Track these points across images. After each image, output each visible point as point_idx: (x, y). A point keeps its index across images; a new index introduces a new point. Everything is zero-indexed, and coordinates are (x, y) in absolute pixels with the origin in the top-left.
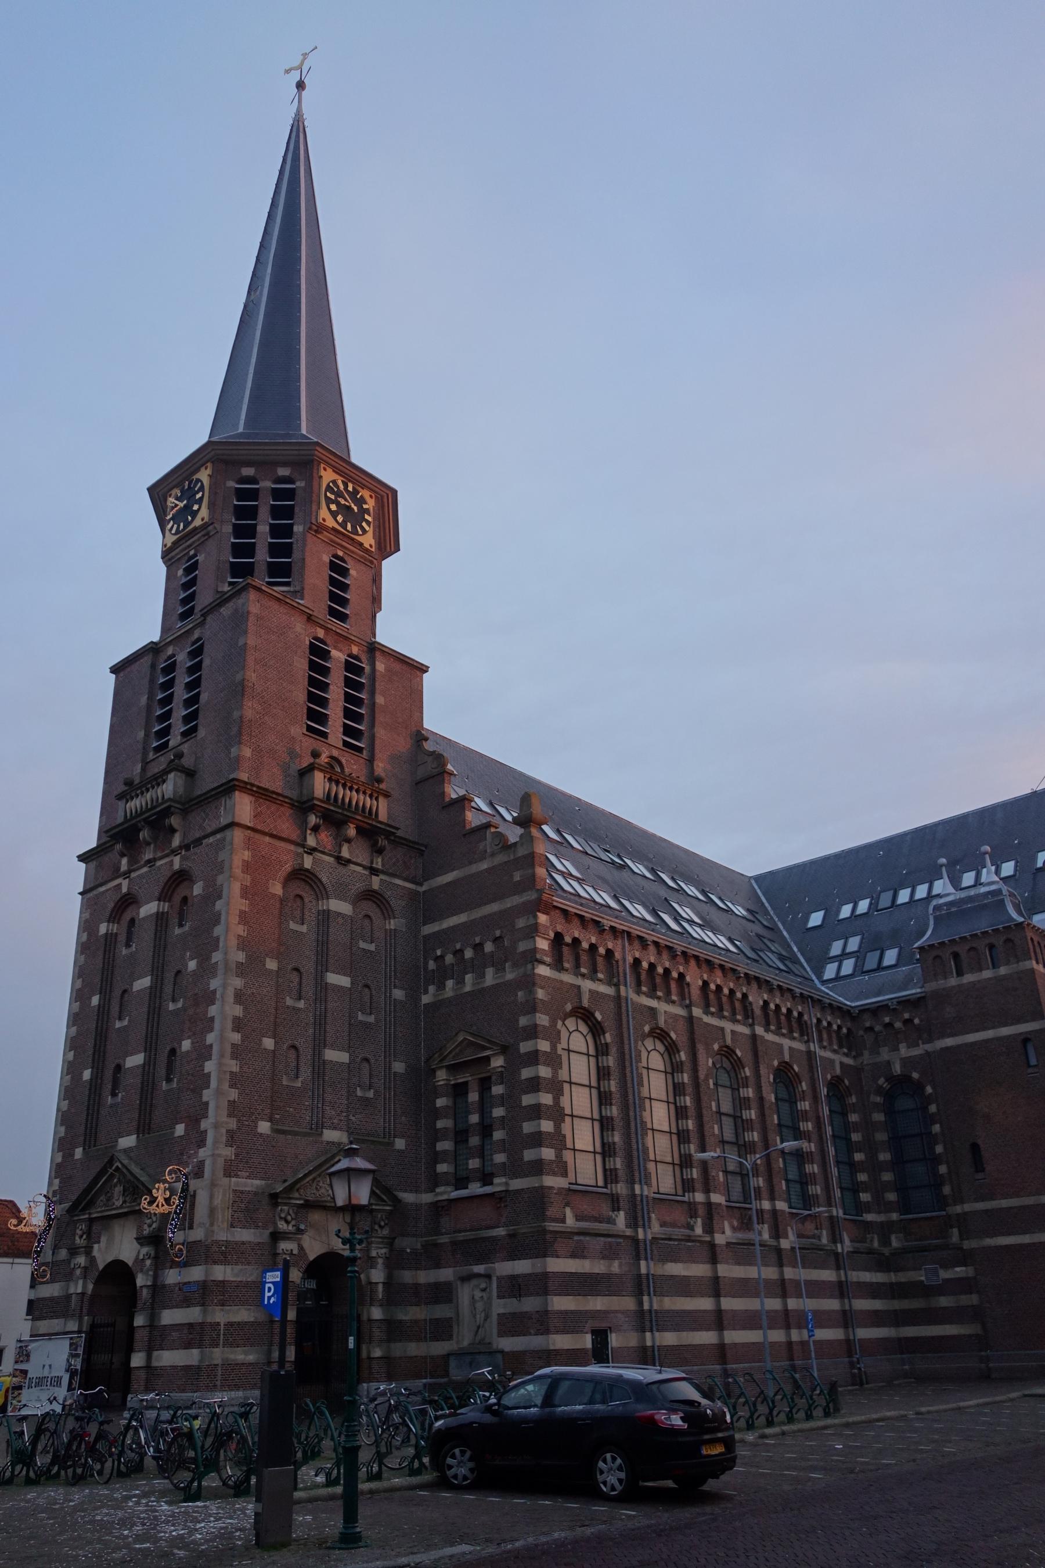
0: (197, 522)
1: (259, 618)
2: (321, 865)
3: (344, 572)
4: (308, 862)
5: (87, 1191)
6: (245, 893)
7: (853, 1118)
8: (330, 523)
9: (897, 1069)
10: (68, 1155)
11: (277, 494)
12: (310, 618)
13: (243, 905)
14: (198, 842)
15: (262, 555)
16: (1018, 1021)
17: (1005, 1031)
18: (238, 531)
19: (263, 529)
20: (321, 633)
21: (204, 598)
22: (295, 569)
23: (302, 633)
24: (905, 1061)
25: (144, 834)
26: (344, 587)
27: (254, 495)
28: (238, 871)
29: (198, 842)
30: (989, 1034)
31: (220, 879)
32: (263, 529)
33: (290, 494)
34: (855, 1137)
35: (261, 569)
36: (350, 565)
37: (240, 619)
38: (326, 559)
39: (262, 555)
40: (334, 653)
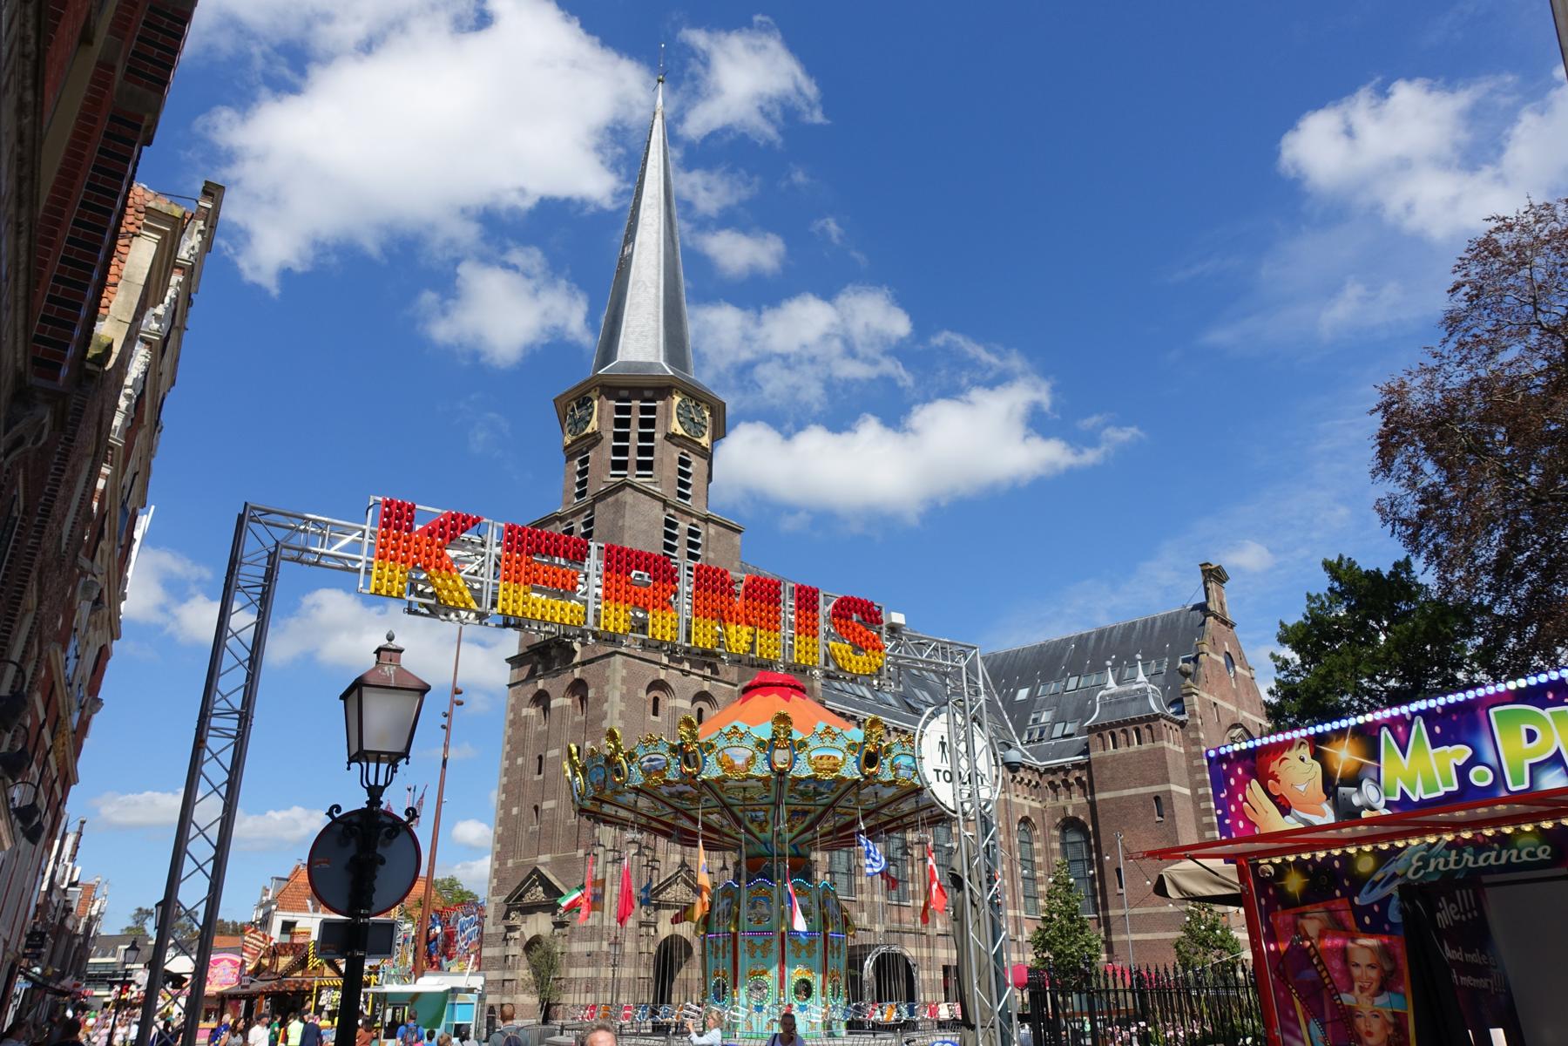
0: (589, 430)
1: (633, 506)
2: (671, 676)
3: (686, 463)
4: (662, 675)
5: (519, 888)
6: (623, 697)
7: (1037, 845)
8: (680, 431)
9: (1070, 813)
10: (503, 864)
11: (644, 410)
12: (666, 504)
13: (622, 706)
14: (591, 661)
15: (633, 456)
16: (1152, 783)
17: (1142, 790)
18: (618, 437)
19: (634, 436)
20: (672, 512)
21: (594, 488)
22: (655, 466)
23: (658, 513)
24: (1075, 807)
25: (553, 652)
26: (687, 475)
27: (627, 410)
28: (618, 684)
29: (591, 661)
30: (1132, 791)
31: (607, 688)
32: (634, 436)
33: (652, 410)
34: (1038, 859)
35: (632, 466)
36: (693, 458)
37: (620, 507)
38: (676, 456)
39: (633, 456)
40: (681, 524)
